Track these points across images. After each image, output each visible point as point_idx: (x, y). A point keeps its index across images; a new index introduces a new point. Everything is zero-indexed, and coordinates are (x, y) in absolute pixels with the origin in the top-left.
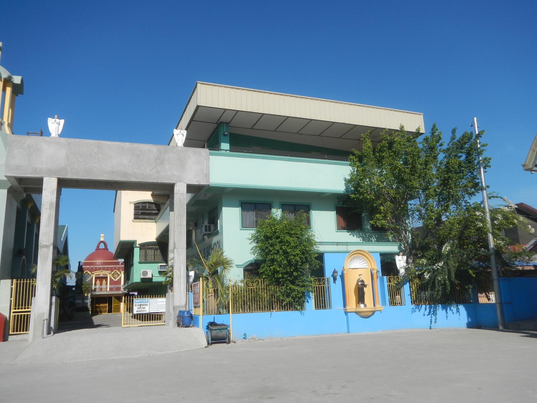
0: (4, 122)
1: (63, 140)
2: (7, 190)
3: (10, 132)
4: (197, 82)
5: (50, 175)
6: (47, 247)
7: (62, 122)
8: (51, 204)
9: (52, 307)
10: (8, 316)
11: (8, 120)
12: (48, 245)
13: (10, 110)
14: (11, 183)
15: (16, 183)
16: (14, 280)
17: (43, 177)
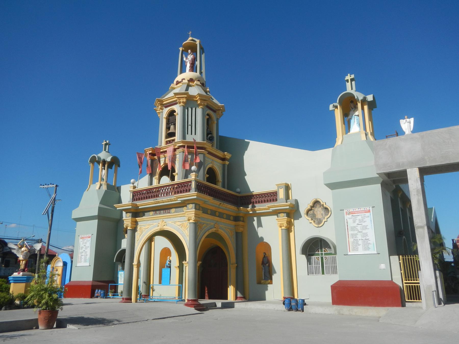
0: (368, 133)
1: (416, 135)
2: (380, 184)
3: (373, 140)
5: (412, 166)
6: (422, 227)
7: (412, 120)
8: (418, 191)
9: (438, 280)
10: (401, 286)
11: (370, 131)
12: (423, 225)
13: (370, 122)
14: (382, 178)
15: (386, 178)
16: (400, 256)
17: (406, 169)
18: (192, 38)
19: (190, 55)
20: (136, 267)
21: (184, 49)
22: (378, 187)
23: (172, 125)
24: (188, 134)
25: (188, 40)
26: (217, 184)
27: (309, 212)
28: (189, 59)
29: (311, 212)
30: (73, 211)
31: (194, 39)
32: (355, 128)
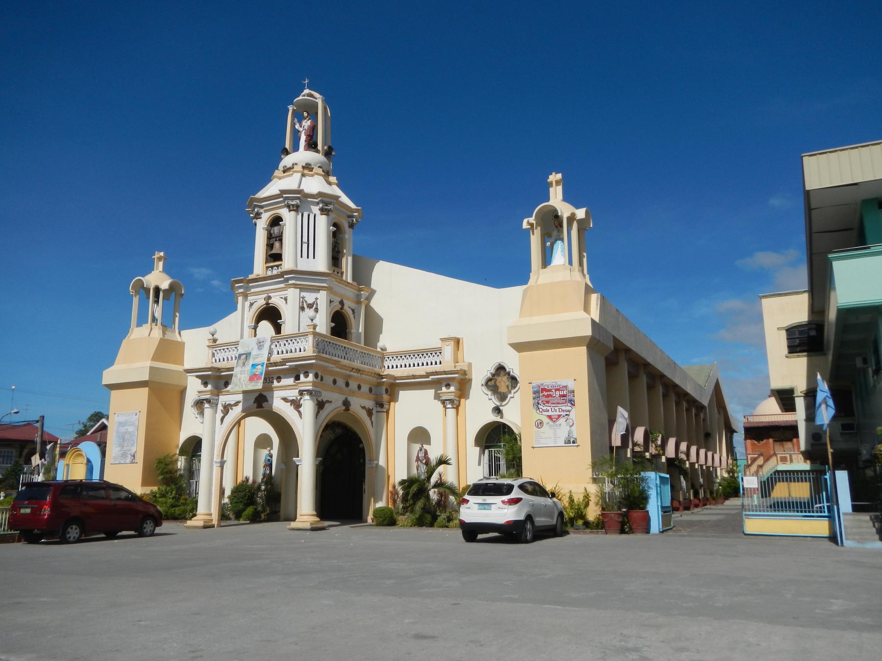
2: (585, 348)
4: (803, 155)
18: (310, 91)
19: (306, 121)
20: (220, 466)
21: (295, 108)
22: (583, 350)
23: (276, 240)
24: (301, 257)
25: (303, 93)
26: (348, 338)
27: (489, 383)
28: (303, 127)
29: (493, 382)
30: (105, 372)
31: (313, 92)
32: (559, 256)
